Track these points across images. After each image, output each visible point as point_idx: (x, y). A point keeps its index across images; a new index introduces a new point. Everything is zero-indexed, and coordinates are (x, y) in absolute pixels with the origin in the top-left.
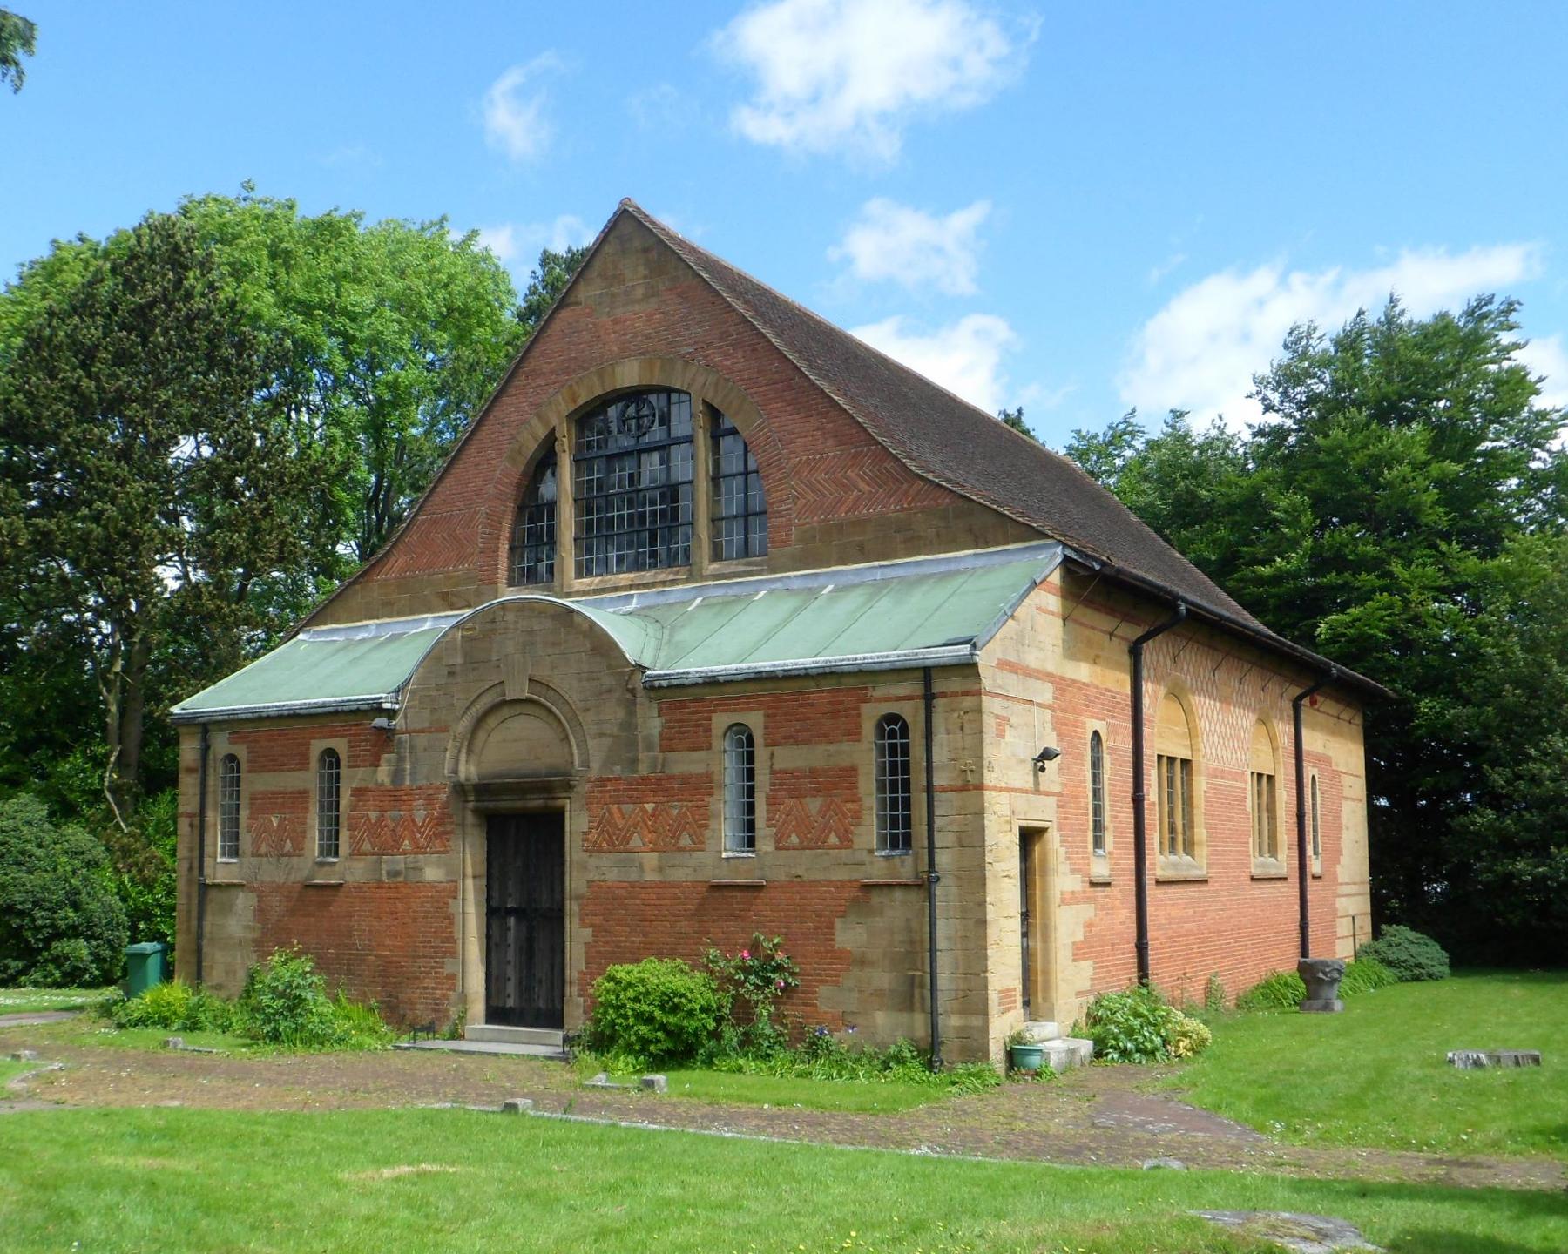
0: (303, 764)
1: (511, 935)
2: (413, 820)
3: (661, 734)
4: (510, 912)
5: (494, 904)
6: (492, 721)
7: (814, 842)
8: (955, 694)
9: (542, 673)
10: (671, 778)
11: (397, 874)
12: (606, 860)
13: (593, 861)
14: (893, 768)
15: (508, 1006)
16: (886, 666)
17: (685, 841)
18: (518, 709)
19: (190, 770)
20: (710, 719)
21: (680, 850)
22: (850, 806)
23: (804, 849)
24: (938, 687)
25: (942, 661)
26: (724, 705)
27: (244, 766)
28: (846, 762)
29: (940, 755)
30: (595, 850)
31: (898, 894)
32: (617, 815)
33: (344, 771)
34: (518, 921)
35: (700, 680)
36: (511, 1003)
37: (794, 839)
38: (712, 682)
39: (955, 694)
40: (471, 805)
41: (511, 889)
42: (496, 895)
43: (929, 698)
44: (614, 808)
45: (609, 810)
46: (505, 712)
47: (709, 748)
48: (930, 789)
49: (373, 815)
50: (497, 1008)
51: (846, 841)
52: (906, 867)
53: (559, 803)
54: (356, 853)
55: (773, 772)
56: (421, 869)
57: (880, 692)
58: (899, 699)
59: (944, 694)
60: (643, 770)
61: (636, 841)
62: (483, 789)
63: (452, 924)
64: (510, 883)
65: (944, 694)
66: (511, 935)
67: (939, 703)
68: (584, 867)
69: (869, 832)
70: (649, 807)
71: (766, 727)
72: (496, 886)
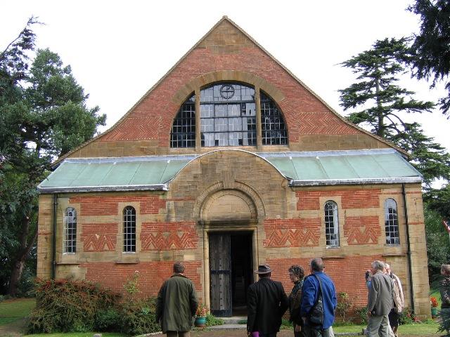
0: (114, 211)
1: (222, 282)
2: (177, 236)
3: (297, 203)
4: (221, 272)
5: (213, 269)
6: (215, 197)
7: (362, 240)
8: (412, 193)
9: (242, 179)
10: (303, 219)
11: (169, 258)
12: (274, 251)
13: (268, 251)
14: (391, 217)
15: (221, 309)
16: (391, 182)
17: (310, 243)
18: (228, 192)
19: (46, 214)
20: (318, 199)
21: (309, 246)
22: (376, 229)
23: (360, 244)
24: (407, 190)
25: (411, 182)
26: (324, 193)
27: (79, 213)
28: (374, 214)
29: (409, 213)
30: (270, 246)
31: (396, 259)
32: (279, 234)
33: (138, 215)
34: (225, 277)
35: (318, 184)
36: (222, 308)
37: (355, 241)
38: (323, 185)
39: (412, 193)
40: (207, 230)
41: (220, 263)
42: (213, 265)
43: (403, 194)
44: (278, 231)
45: (275, 231)
46: (221, 193)
47: (319, 209)
48: (407, 224)
49: (155, 235)
50: (215, 311)
51: (375, 242)
52: (398, 250)
53: (252, 229)
54: (145, 249)
55: (346, 218)
56: (182, 256)
57: (386, 191)
58: (392, 194)
59: (408, 193)
60: (290, 217)
61: (288, 243)
62: (213, 224)
63: (199, 278)
64: (220, 261)
65: (408, 193)
66: (222, 282)
67: (408, 196)
68: (264, 253)
69: (383, 238)
70: (294, 230)
71: (342, 202)
72: (213, 262)
